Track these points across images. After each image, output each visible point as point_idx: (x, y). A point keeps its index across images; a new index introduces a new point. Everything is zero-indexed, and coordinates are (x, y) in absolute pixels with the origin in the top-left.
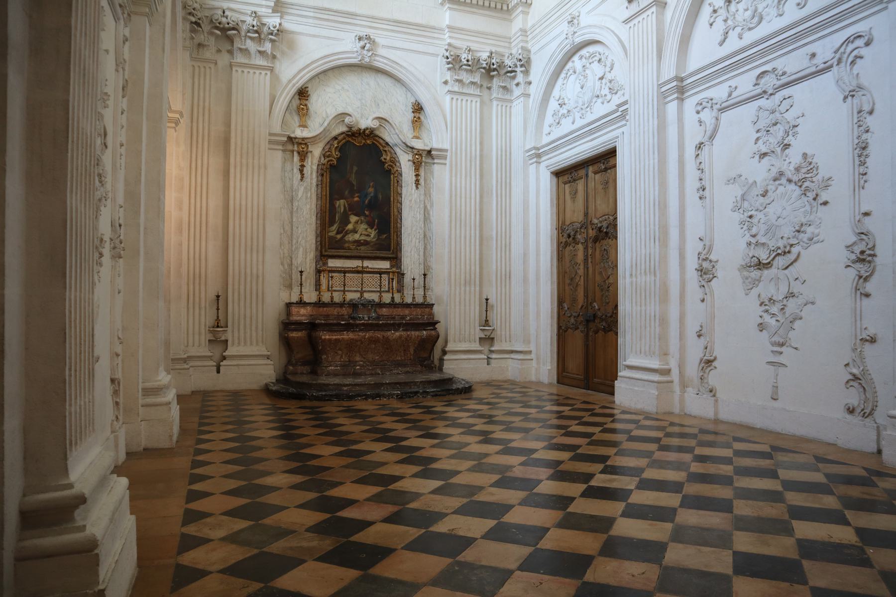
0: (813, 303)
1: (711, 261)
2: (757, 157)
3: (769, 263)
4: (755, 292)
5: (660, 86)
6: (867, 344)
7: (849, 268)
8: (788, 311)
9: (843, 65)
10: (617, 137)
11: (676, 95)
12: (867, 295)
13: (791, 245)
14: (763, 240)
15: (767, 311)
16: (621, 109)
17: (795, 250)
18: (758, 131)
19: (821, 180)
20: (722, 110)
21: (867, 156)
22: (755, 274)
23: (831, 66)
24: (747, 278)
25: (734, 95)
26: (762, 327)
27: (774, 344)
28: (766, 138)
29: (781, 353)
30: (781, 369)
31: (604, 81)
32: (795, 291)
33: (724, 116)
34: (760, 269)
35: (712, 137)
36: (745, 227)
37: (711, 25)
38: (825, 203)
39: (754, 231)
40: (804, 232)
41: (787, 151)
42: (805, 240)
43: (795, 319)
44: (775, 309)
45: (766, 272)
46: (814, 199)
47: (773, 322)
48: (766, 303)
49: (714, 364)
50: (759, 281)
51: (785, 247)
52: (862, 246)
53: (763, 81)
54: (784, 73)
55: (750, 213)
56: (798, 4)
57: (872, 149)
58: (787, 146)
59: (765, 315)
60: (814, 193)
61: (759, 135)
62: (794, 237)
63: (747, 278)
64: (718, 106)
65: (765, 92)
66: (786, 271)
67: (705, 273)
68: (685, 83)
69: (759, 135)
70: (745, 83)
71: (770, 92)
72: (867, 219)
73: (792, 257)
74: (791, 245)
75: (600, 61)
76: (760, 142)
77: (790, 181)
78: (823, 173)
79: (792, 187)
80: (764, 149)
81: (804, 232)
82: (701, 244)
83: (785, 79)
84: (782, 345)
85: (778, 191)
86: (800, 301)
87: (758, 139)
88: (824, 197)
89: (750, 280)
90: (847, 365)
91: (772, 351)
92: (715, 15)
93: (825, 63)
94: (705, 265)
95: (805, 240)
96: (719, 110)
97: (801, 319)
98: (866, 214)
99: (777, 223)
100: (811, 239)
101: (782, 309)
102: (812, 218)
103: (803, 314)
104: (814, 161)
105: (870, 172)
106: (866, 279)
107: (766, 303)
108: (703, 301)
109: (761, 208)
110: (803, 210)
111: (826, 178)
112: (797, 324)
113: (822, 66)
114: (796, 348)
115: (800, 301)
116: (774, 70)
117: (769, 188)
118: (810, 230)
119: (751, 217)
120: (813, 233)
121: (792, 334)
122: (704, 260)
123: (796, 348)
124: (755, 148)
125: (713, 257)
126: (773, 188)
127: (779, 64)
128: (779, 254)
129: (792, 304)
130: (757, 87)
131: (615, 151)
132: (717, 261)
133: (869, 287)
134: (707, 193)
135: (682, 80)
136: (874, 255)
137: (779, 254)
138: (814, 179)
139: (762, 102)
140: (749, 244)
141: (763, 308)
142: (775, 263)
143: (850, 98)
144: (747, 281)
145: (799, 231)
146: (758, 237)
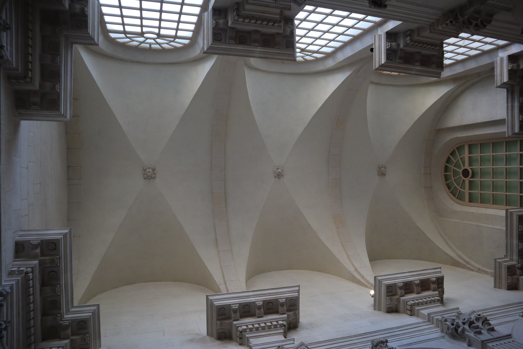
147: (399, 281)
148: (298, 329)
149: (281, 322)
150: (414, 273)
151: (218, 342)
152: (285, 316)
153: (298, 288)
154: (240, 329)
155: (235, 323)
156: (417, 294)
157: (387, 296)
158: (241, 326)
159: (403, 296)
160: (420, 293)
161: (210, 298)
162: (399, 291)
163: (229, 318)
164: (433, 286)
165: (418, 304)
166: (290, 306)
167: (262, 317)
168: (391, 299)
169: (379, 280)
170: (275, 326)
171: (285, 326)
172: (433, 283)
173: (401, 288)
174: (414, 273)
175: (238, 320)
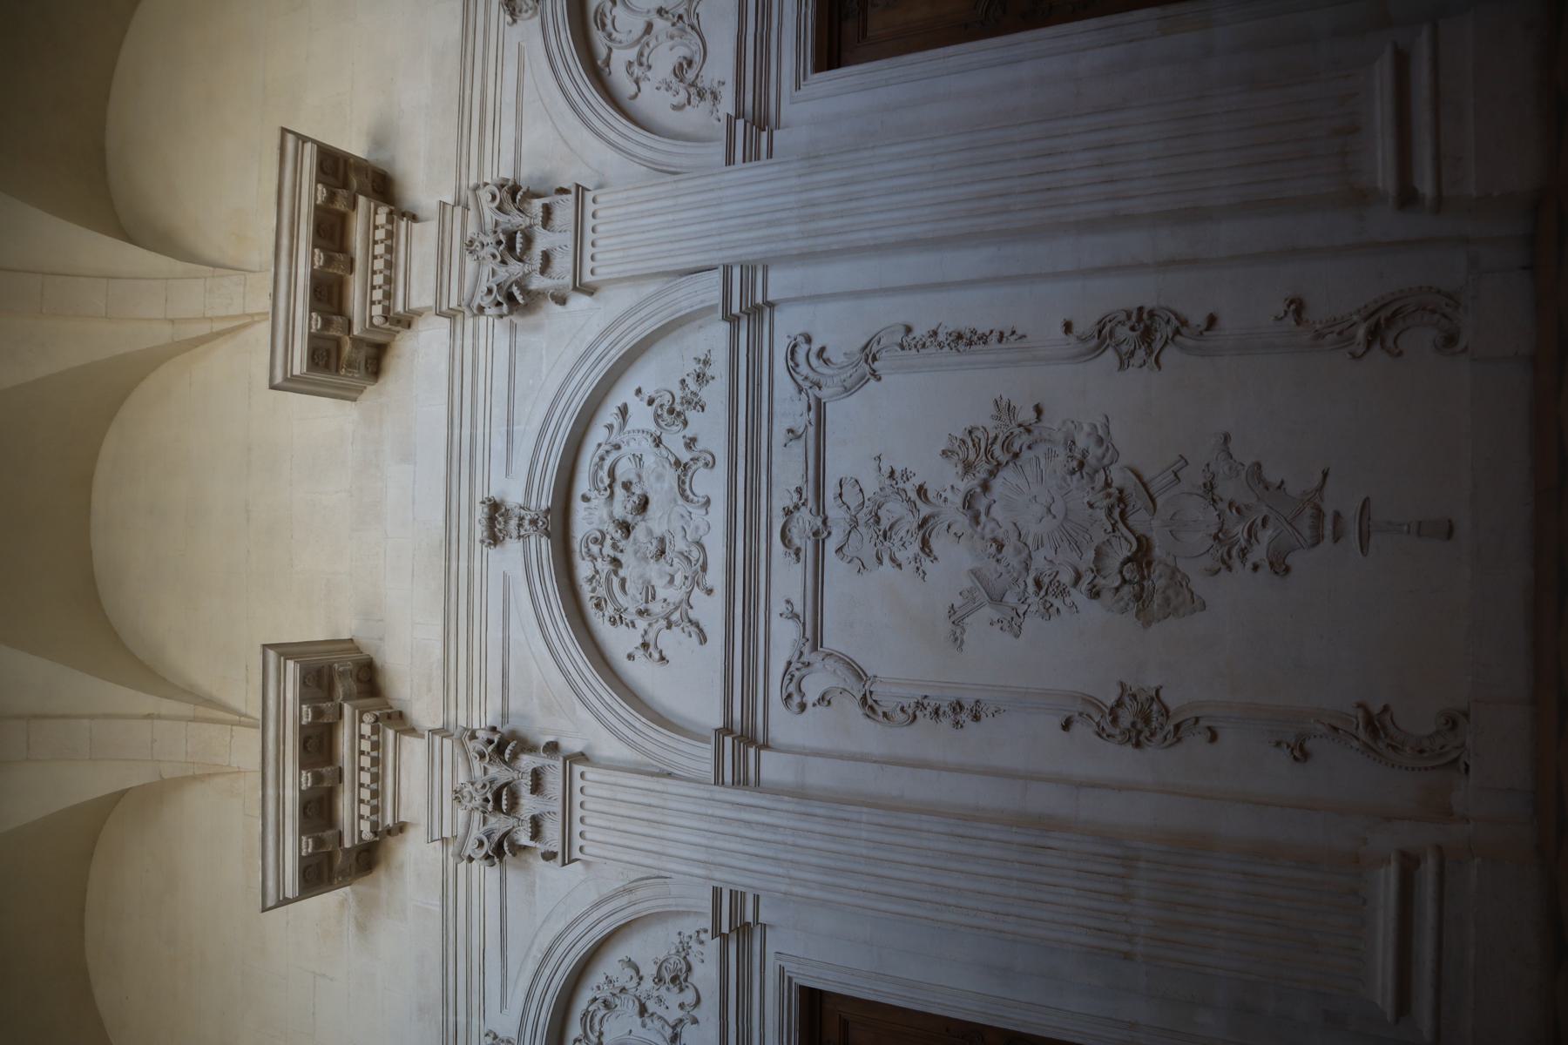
0: (1227, 438)
1: (1120, 703)
2: (927, 564)
3: (1138, 539)
4: (1200, 585)
5: (719, 780)
6: (1305, 316)
7: (1162, 359)
9: (823, 382)
10: (782, 969)
11: (752, 751)
12: (1212, 321)
13: (1108, 484)
14: (1091, 555)
15: (1244, 553)
16: (725, 929)
17: (1117, 477)
18: (880, 560)
19: (995, 423)
20: (816, 642)
21: (974, 332)
22: (1158, 579)
23: (818, 400)
25: (798, 609)
26: (1279, 566)
27: (1318, 539)
28: (898, 543)
29: (1337, 516)
31: (651, 1006)
33: (830, 642)
34: (1149, 564)
35: (859, 674)
36: (1057, 603)
37: (662, 658)
38: (1038, 410)
39: (1066, 577)
40: (1085, 453)
41: (931, 495)
42: (1100, 452)
43: (1261, 479)
44: (1239, 531)
45: (1157, 552)
46: (1029, 431)
47: (1265, 536)
48: (1227, 551)
49: (1376, 709)
50: (1175, 571)
51: (1109, 495)
52: (1123, 332)
53: (797, 542)
54: (799, 491)
55: (1031, 588)
56: (706, 464)
57: (963, 324)
58: (921, 491)
60: (1017, 431)
61: (886, 560)
62: (1092, 478)
63: (1167, 600)
64: (806, 650)
65: (816, 534)
66: (1159, 501)
67: (1147, 721)
68: (737, 728)
69: (886, 560)
70: (787, 580)
71: (819, 522)
72: (1078, 329)
73: (1130, 484)
74: (1108, 484)
75: (606, 1004)
76: (900, 556)
77: (985, 487)
78: (984, 418)
79: (997, 485)
80: (915, 547)
81: (1085, 453)
82: (1077, 728)
83: (809, 493)
84: (1319, 514)
85: (999, 519)
87: (893, 560)
88: (1027, 415)
89: (1170, 592)
90: (1354, 356)
91: (1336, 539)
92: (651, 649)
93: (809, 409)
94: (1126, 718)
96: (815, 649)
97: (1259, 465)
98: (1068, 327)
99: (1060, 517)
100: (1100, 441)
102: (1059, 437)
103: (1247, 464)
104: (959, 436)
105: (998, 327)
106: (1184, 323)
107: (1227, 551)
108: (1214, 737)
109: (1024, 555)
110: (1043, 461)
111: (995, 413)
112: (1272, 475)
113: (812, 414)
114: (1325, 475)
116: (788, 512)
117: (988, 536)
118: (1082, 441)
119: (1038, 584)
120: (1089, 435)
122: (1115, 721)
123: (1325, 475)
124: (909, 568)
125: (1110, 701)
126: (993, 524)
127: (782, 499)
128: (1123, 514)
129: (1228, 490)
130: (802, 555)
131: (812, 991)
132: (1122, 685)
133: (1197, 318)
134: (968, 700)
135: (726, 730)
136: (1140, 309)
137: (1123, 514)
138: (992, 435)
139: (831, 545)
140: (1095, 594)
141: (1236, 563)
142: (1140, 530)
143: (876, 365)
145: (1081, 465)
146: (1082, 567)
147: (303, 320)
148: (378, 662)
149: (366, 729)
150: (285, 241)
151: (380, 874)
152: (347, 709)
153: (272, 654)
154: (367, 835)
155: (347, 845)
156: (351, 270)
157: (337, 371)
158: (360, 832)
159: (350, 323)
160: (352, 261)
161: (270, 902)
162: (333, 333)
163: (330, 856)
164: (340, 206)
165: (388, 296)
166: (319, 686)
167: (341, 771)
168: (350, 365)
169: (286, 379)
170: (375, 746)
171: (377, 719)
172: (331, 197)
173: (327, 323)
174: (285, 241)
175: (340, 834)
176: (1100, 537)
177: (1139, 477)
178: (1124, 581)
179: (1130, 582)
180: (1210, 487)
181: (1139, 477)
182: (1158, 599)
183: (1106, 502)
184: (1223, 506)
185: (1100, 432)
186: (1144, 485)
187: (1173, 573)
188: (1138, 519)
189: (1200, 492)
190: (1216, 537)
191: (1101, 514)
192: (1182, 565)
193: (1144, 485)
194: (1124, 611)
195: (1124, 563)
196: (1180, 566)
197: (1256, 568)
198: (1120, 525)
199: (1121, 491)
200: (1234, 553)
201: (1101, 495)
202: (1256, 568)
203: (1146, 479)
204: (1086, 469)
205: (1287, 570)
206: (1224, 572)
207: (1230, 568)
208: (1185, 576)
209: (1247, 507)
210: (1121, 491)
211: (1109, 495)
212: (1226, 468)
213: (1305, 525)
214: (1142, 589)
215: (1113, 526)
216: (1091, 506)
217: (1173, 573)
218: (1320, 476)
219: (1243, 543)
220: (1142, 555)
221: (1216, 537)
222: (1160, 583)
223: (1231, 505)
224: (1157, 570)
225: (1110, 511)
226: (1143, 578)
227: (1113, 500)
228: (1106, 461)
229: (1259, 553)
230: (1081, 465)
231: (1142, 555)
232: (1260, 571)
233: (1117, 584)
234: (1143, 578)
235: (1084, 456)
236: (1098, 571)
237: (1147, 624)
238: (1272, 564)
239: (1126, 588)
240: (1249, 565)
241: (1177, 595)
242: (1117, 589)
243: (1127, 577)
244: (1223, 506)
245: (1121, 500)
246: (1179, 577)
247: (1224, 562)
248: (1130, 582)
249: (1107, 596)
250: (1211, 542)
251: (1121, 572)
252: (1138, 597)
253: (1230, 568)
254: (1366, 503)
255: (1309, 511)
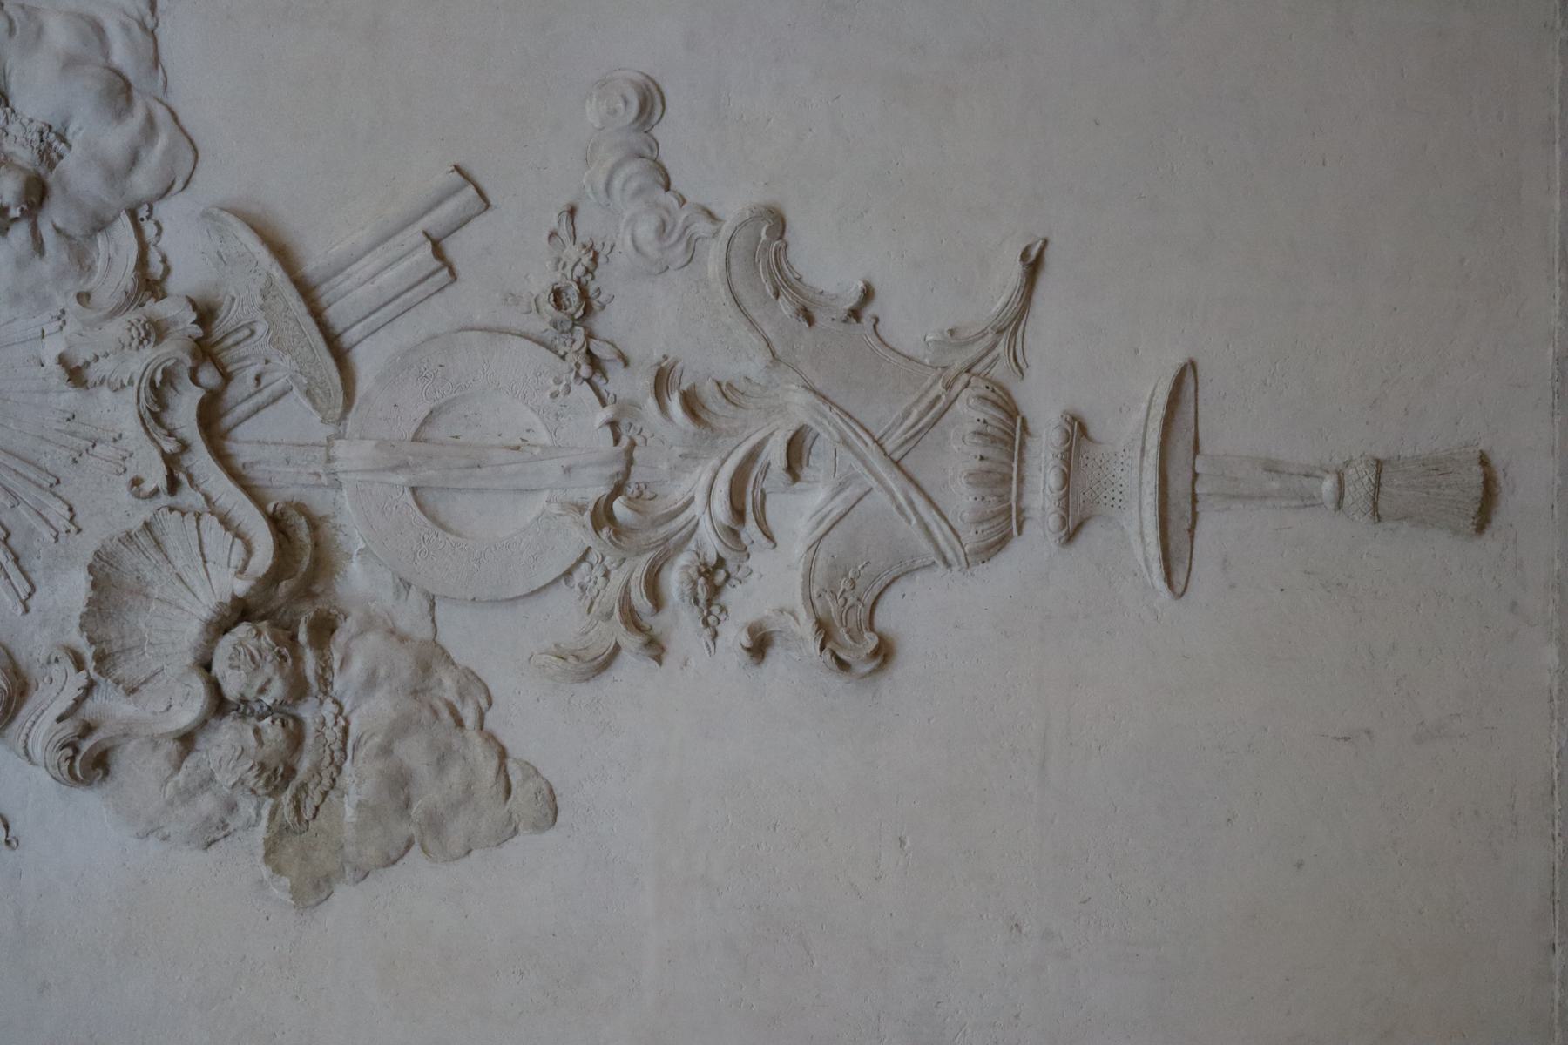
0: (649, 102)
3: (277, 522)
8: (720, 350)
13: (149, 285)
14: (74, 588)
15: (712, 580)
17: (192, 254)
22: (362, 692)
24: (400, 784)
26: (856, 641)
27: (1003, 526)
29: (1077, 431)
30: (1230, 430)
32: (540, 282)
34: (324, 629)
42: (116, 139)
43: (783, 281)
44: (695, 490)
45: (359, 581)
47: (798, 512)
50: (430, 658)
51: (156, 331)
59: (747, 603)
62: (81, 259)
63: (400, 784)
66: (367, 362)
74: (149, 285)
84: (1009, 430)
86: (627, 227)
89: (414, 753)
91: (1071, 532)
95: (116, 139)
97: (777, 222)
100: (119, 93)
101: (691, 404)
103: (733, 209)
112: (828, 267)
114: (1033, 267)
115: (627, 227)
120: (70, 63)
121: (912, 322)
123: (1033, 267)
129: (654, 317)
137: (210, 415)
140: (88, 760)
142: (287, 481)
144: (429, 794)
145: (37, 193)
176: (111, 510)
177: (282, 253)
178: (219, 704)
179: (243, 708)
180: (577, 305)
181: (282, 253)
182: (360, 782)
183: (141, 362)
184: (630, 385)
185: (120, 55)
186: (306, 290)
187: (425, 668)
188: (280, 435)
189: (540, 325)
190: (602, 516)
191: (119, 412)
192: (462, 634)
193: (306, 290)
194: (212, 835)
195: (220, 626)
196: (448, 638)
197: (759, 646)
198: (201, 460)
199: (206, 314)
200: (674, 581)
201: (118, 329)
202: (759, 646)
203: (312, 266)
204: (54, 215)
205: (884, 653)
206: (633, 662)
207: (655, 647)
208: (472, 681)
209: (727, 391)
210: (206, 314)
211: (156, 331)
212: (646, 230)
213: (954, 464)
214: (296, 739)
215: (171, 461)
216: (76, 375)
217: (425, 668)
218: (1014, 272)
219: (711, 544)
220: (292, 596)
221: (602, 516)
222: (372, 714)
223: (662, 381)
224: (357, 655)
225: (158, 393)
226: (298, 689)
227: (174, 350)
228: (142, 183)
229: (771, 585)
230: (37, 193)
231: (292, 596)
232: (776, 654)
233: (187, 713)
234: (298, 689)
235: (47, 156)
236: (101, 659)
237: (314, 889)
238: (824, 629)
239: (228, 736)
240: (734, 635)
241: (442, 760)
242: (187, 740)
243: (231, 690)
244: (630, 385)
245: (205, 351)
246: (447, 685)
247: (632, 619)
248: (243, 708)
249: (142, 770)
250: (579, 534)
251: (206, 666)
252: (278, 776)
253: (655, 647)
254: (1184, 382)
255: (969, 412)
